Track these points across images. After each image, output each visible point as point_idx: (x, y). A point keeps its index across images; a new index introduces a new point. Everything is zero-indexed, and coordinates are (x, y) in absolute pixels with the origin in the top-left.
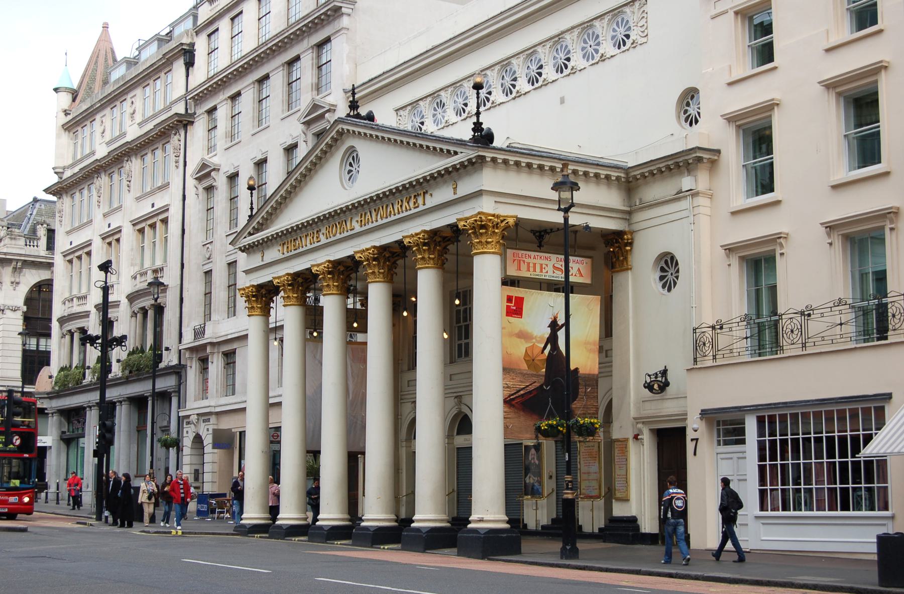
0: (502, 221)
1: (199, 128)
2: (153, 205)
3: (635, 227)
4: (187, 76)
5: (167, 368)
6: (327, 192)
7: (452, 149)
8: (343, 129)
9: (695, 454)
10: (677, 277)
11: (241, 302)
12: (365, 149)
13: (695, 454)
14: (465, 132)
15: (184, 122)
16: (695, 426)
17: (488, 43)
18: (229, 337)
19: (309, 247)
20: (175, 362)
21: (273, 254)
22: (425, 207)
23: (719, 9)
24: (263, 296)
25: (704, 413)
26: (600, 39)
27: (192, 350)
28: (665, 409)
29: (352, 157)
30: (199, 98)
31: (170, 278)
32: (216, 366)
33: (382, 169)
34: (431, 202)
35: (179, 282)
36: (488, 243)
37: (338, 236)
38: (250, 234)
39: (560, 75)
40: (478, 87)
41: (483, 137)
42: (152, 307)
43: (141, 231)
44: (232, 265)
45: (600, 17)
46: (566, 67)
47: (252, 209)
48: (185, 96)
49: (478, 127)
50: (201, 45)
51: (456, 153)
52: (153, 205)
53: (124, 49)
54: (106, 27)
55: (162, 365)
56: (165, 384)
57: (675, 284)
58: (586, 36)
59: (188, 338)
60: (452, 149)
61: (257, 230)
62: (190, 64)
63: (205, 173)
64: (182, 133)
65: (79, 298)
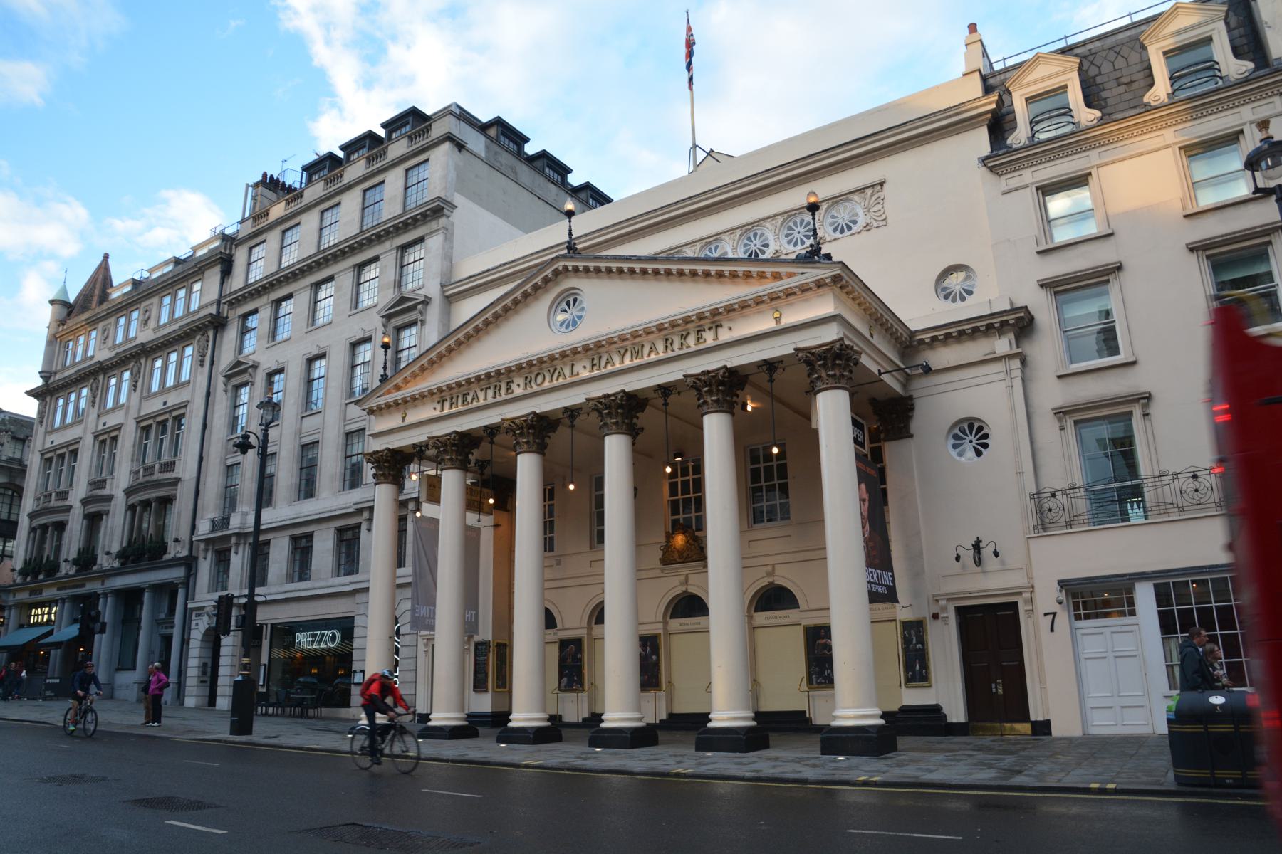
1: (231, 334)
2: (165, 403)
5: (175, 559)
8: (566, 268)
9: (1052, 630)
11: (369, 471)
13: (1052, 630)
15: (217, 323)
17: (647, 235)
20: (185, 553)
24: (393, 465)
27: (207, 541)
28: (989, 584)
29: (570, 300)
30: (235, 302)
31: (186, 469)
34: (725, 336)
35: (195, 475)
36: (842, 376)
37: (547, 384)
38: (389, 392)
42: (153, 500)
43: (147, 429)
47: (385, 368)
48: (218, 302)
50: (240, 256)
52: (165, 403)
53: (121, 275)
54: (106, 256)
55: (166, 557)
56: (177, 574)
58: (751, 235)
59: (204, 528)
62: (227, 272)
64: (211, 334)
65: (58, 494)
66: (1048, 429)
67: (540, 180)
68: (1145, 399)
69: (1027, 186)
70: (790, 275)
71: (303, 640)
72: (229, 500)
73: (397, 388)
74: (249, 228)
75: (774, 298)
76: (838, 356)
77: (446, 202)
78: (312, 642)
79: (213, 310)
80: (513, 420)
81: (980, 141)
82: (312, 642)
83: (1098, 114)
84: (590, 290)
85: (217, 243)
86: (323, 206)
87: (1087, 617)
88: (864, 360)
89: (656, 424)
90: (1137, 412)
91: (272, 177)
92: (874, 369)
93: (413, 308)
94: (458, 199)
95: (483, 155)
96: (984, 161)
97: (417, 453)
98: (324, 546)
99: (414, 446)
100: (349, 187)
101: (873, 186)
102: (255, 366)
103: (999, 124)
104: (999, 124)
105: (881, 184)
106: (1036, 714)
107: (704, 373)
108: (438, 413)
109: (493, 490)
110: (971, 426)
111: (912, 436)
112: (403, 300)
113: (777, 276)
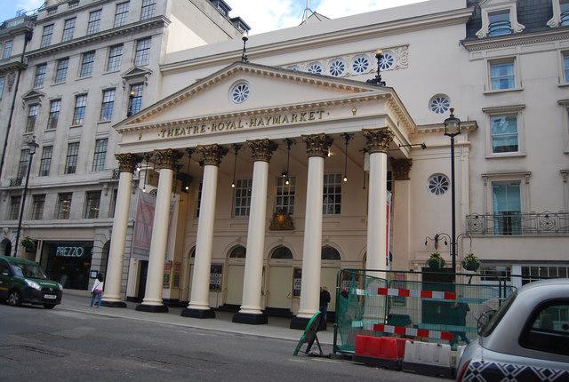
1: (29, 75)
3: (414, 158)
4: (26, 45)
8: (241, 69)
15: (21, 68)
24: (129, 162)
32: (29, 201)
34: (325, 117)
38: (133, 122)
40: (379, 57)
44: (101, 141)
50: (38, 32)
60: (361, 87)
62: (28, 38)
63: (33, 98)
64: (17, 73)
66: (479, 186)
67: (216, 13)
68: (528, 175)
69: (483, 59)
70: (364, 91)
71: (62, 251)
72: (25, 169)
73: (138, 121)
74: (44, 15)
75: (353, 101)
78: (67, 253)
79: (19, 60)
80: (204, 147)
81: (461, 32)
82: (67, 253)
83: (524, 27)
84: (254, 83)
85: (22, 21)
86: (91, 10)
88: (395, 139)
89: (285, 158)
90: (523, 182)
92: (397, 143)
94: (172, 18)
96: (462, 42)
97: (147, 157)
98: (78, 200)
99: (145, 153)
103: (473, 24)
104: (473, 24)
105: (407, 46)
107: (312, 135)
108: (160, 137)
109: (187, 182)
110: (440, 178)
111: (409, 179)
112: (136, 70)
113: (357, 90)
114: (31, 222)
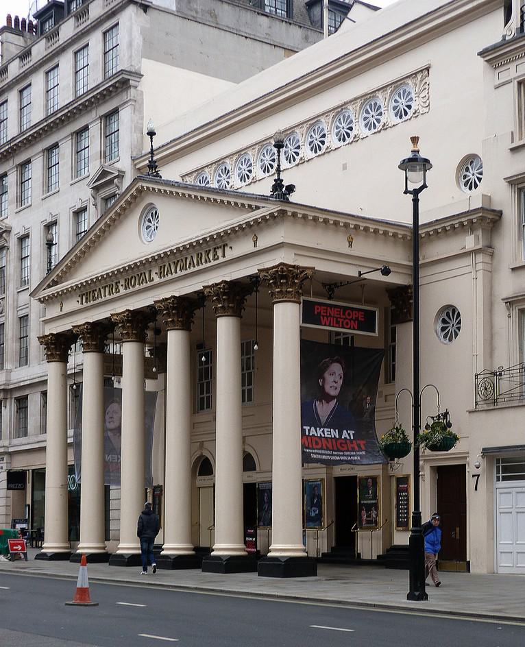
0: (301, 272)
6: (129, 246)
7: (253, 204)
8: (142, 187)
9: (476, 489)
10: (459, 328)
12: (162, 205)
13: (476, 489)
14: (265, 188)
16: (475, 464)
18: (22, 384)
19: (108, 297)
21: (72, 305)
22: (225, 259)
23: (503, 79)
25: (486, 452)
26: (382, 110)
29: (151, 214)
33: (180, 226)
37: (137, 287)
38: (49, 286)
39: (342, 143)
41: (282, 191)
45: (384, 88)
46: (349, 135)
49: (278, 185)
51: (258, 208)
57: (456, 335)
58: (368, 107)
61: (55, 283)
76: (283, 277)
77: (130, 73)
87: (505, 479)
91: (17, 19)
93: (111, 182)
95: (174, 8)
100: (62, 50)
101: (421, 71)
102: (8, 232)
105: (428, 69)
106: (468, 560)
108: (79, 306)
114: (16, 441)
